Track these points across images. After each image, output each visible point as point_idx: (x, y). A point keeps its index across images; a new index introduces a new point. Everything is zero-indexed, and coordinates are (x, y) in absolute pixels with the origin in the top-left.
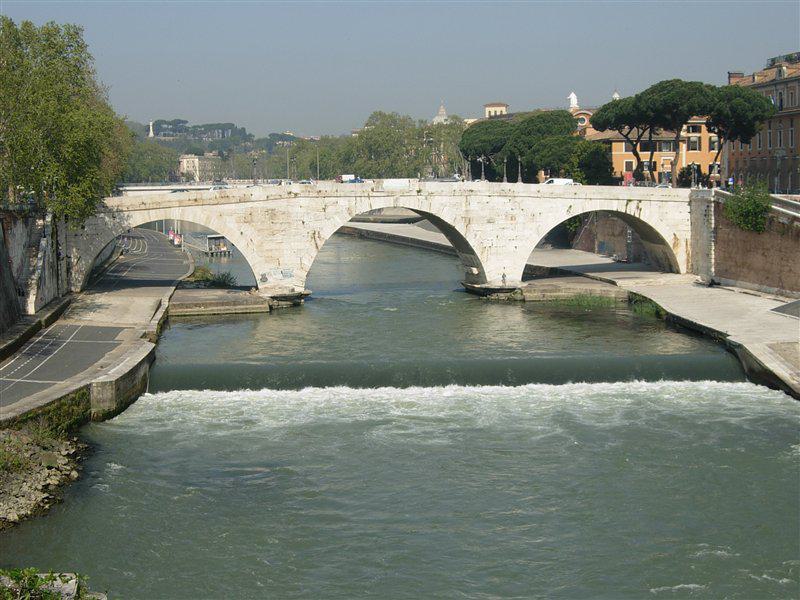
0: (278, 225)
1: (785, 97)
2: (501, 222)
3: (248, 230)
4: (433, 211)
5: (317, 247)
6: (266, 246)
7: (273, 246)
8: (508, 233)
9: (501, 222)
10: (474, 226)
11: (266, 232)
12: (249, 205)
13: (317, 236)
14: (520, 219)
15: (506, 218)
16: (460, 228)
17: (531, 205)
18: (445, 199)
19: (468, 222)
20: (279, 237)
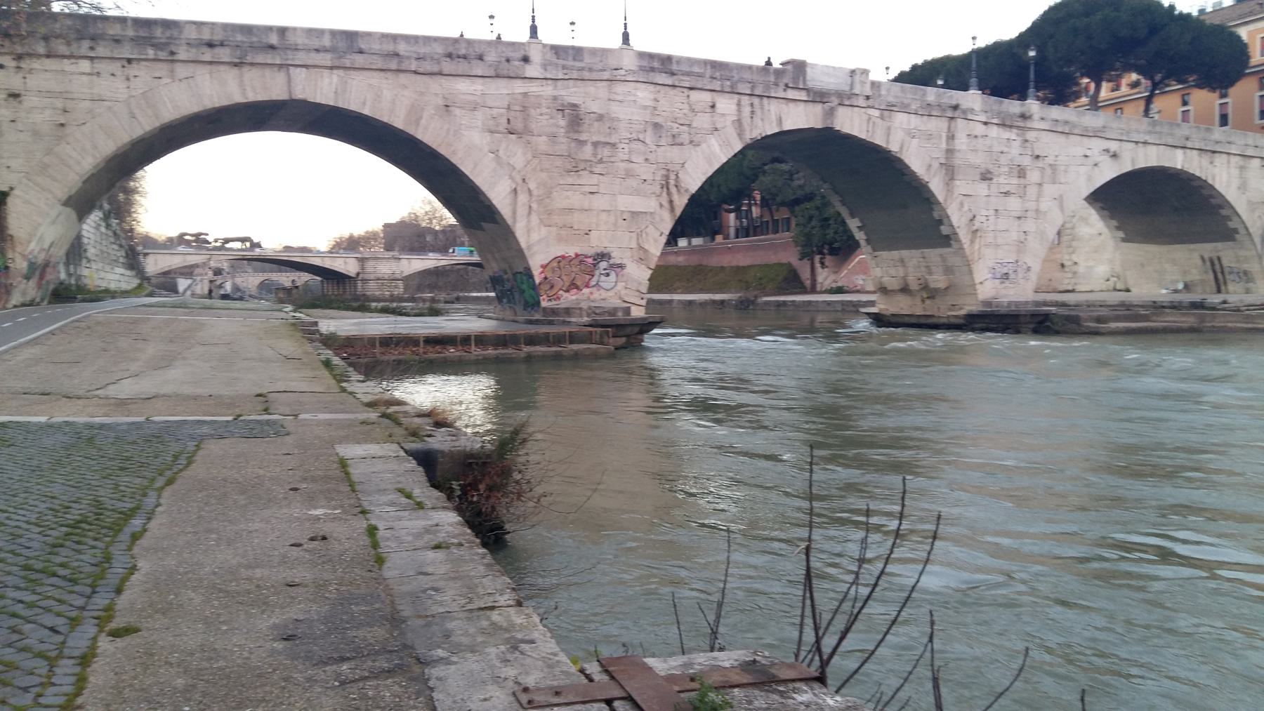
0: (588, 149)
2: (1004, 180)
3: (517, 154)
4: (894, 147)
5: (672, 209)
6: (564, 199)
8: (1014, 204)
9: (1004, 180)
10: (961, 186)
11: (558, 162)
12: (519, 87)
13: (672, 182)
14: (1033, 176)
15: (1009, 174)
17: (1050, 145)
18: (915, 121)
19: (950, 171)
20: (587, 179)
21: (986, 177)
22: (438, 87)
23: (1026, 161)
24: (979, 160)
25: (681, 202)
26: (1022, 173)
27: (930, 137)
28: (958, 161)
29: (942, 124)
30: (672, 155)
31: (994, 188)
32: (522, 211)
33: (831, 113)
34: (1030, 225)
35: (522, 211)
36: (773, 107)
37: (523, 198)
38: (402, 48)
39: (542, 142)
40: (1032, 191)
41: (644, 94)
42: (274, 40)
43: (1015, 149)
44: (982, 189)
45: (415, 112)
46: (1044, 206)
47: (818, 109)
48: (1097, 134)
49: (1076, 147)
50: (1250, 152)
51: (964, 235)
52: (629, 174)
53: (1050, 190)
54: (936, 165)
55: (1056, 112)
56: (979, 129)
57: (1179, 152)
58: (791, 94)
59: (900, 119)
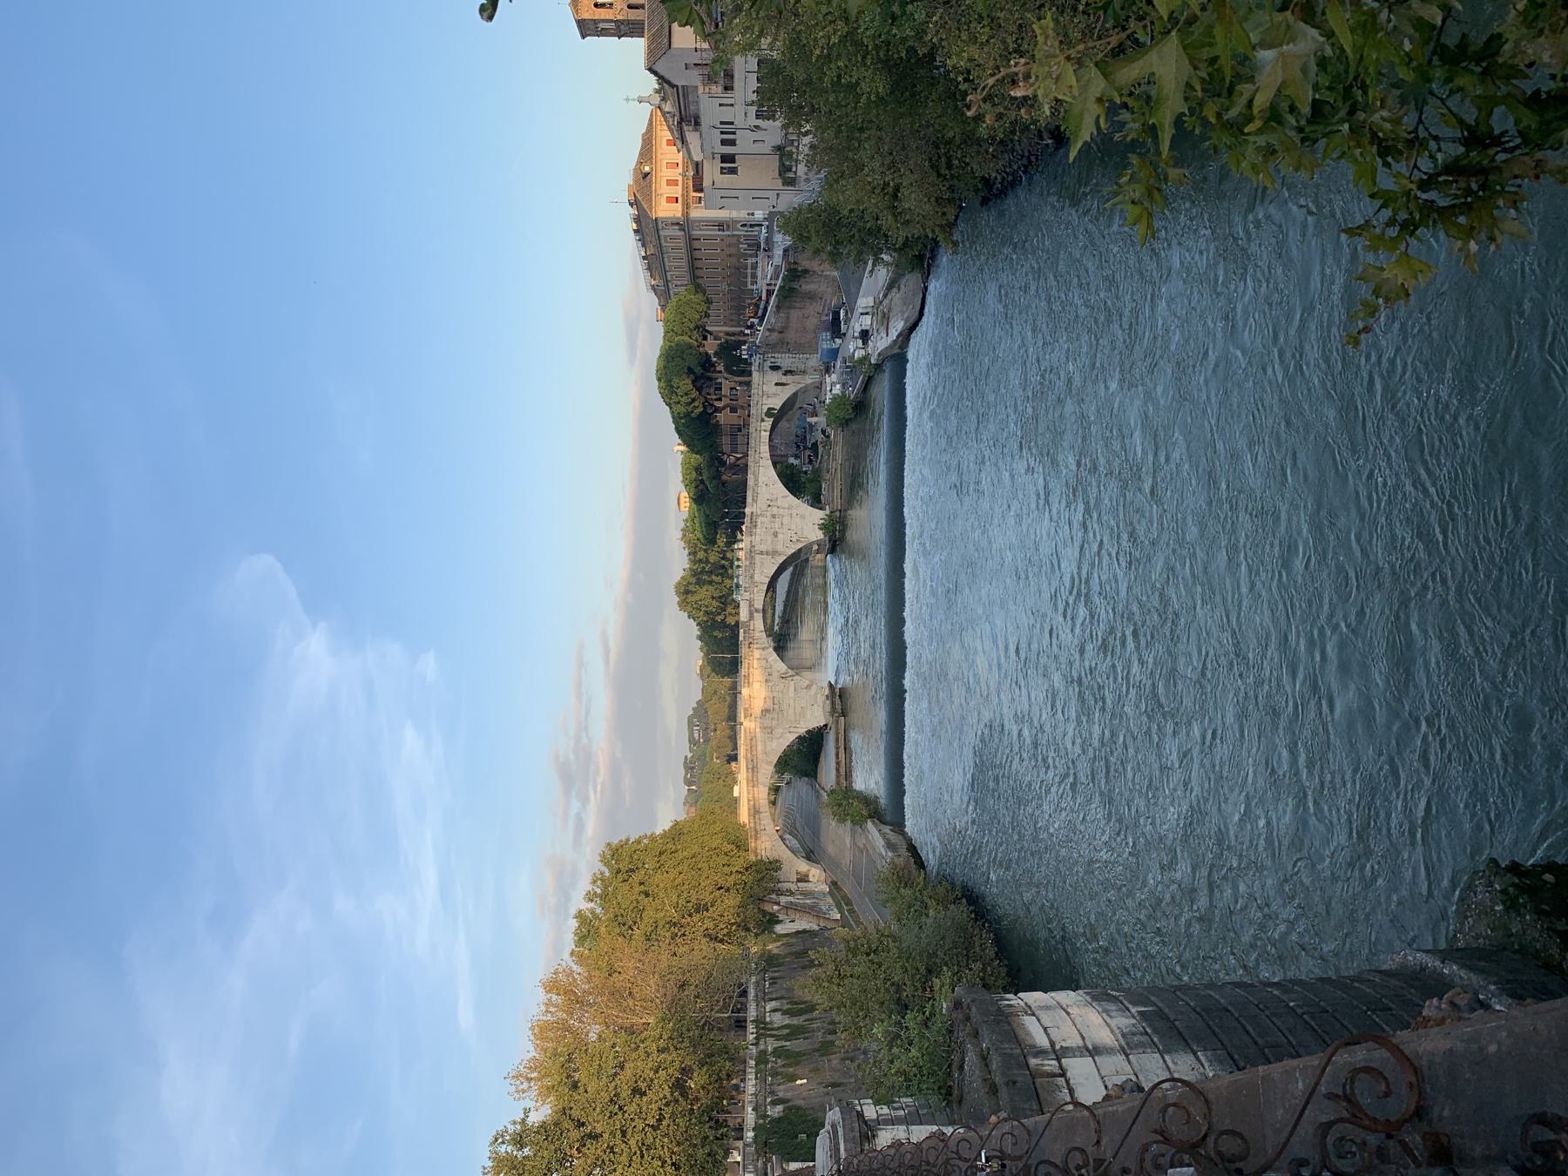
1: (679, 283)
4: (767, 580)
7: (791, 711)
8: (786, 520)
10: (780, 548)
16: (781, 559)
19: (775, 553)
20: (784, 707)
21: (775, 535)
22: (760, 757)
23: (769, 514)
24: (770, 538)
25: (791, 672)
26: (774, 516)
27: (762, 563)
28: (770, 549)
29: (758, 557)
30: (775, 675)
31: (780, 531)
32: (796, 730)
33: (757, 611)
34: (794, 512)
35: (796, 730)
36: (757, 634)
37: (792, 730)
38: (750, 766)
39: (775, 723)
40: (781, 511)
41: (756, 685)
42: (752, 803)
43: (764, 519)
44: (780, 536)
45: (769, 763)
46: (787, 506)
47: (755, 614)
48: (756, 480)
49: (762, 490)
50: (760, 393)
51: (800, 546)
52: (782, 692)
53: (779, 503)
54: (773, 560)
55: (749, 499)
56: (758, 538)
57: (763, 433)
58: (752, 628)
59: (757, 578)
